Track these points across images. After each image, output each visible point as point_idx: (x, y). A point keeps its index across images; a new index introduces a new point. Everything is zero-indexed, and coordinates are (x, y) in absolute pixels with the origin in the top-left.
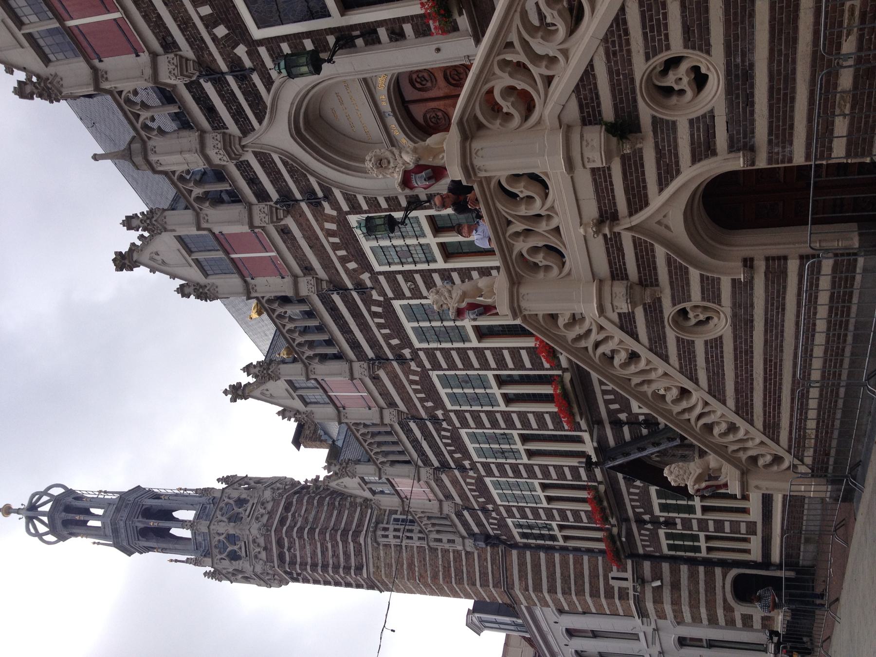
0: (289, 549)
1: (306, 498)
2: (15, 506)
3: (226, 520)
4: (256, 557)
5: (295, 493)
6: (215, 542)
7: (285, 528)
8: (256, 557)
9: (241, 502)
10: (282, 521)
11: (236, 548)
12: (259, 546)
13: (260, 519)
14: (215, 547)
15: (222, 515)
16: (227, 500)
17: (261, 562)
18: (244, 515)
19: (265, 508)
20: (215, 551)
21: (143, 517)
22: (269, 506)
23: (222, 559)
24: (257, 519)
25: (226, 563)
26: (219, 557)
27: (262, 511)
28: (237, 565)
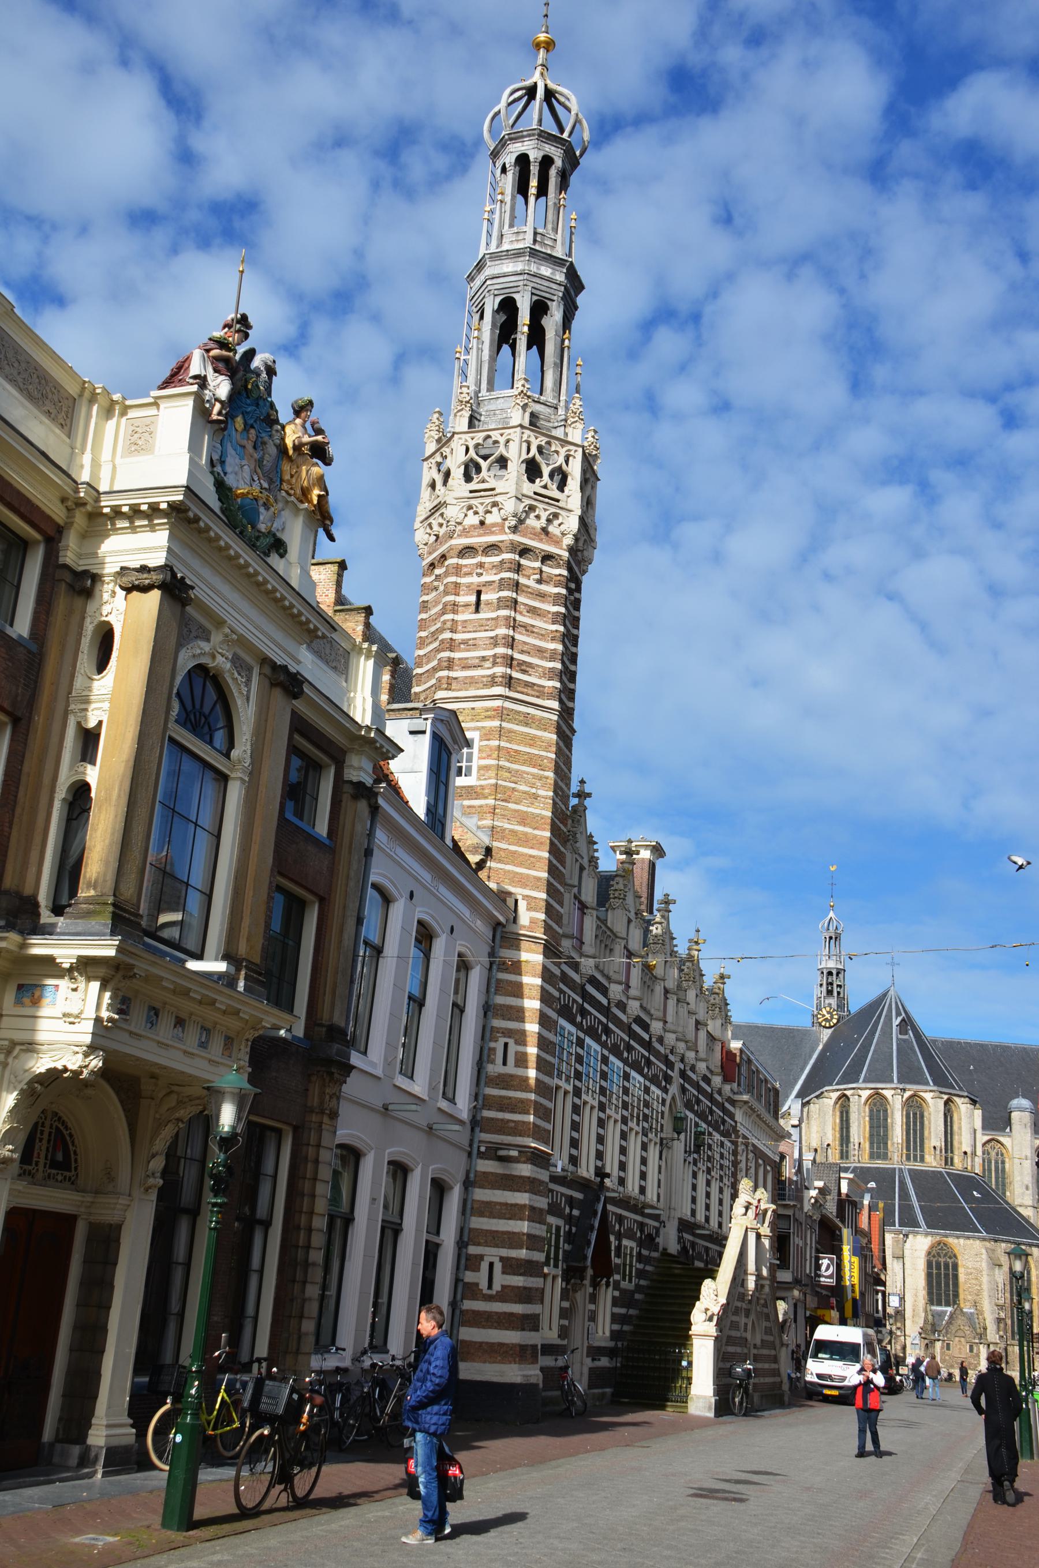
0: (481, 565)
3: (531, 455)
6: (495, 435)
7: (517, 557)
8: (470, 508)
9: (561, 477)
10: (525, 551)
11: (484, 473)
12: (488, 512)
19: (549, 521)
20: (479, 437)
21: (536, 301)
24: (532, 508)
27: (544, 516)
28: (458, 473)
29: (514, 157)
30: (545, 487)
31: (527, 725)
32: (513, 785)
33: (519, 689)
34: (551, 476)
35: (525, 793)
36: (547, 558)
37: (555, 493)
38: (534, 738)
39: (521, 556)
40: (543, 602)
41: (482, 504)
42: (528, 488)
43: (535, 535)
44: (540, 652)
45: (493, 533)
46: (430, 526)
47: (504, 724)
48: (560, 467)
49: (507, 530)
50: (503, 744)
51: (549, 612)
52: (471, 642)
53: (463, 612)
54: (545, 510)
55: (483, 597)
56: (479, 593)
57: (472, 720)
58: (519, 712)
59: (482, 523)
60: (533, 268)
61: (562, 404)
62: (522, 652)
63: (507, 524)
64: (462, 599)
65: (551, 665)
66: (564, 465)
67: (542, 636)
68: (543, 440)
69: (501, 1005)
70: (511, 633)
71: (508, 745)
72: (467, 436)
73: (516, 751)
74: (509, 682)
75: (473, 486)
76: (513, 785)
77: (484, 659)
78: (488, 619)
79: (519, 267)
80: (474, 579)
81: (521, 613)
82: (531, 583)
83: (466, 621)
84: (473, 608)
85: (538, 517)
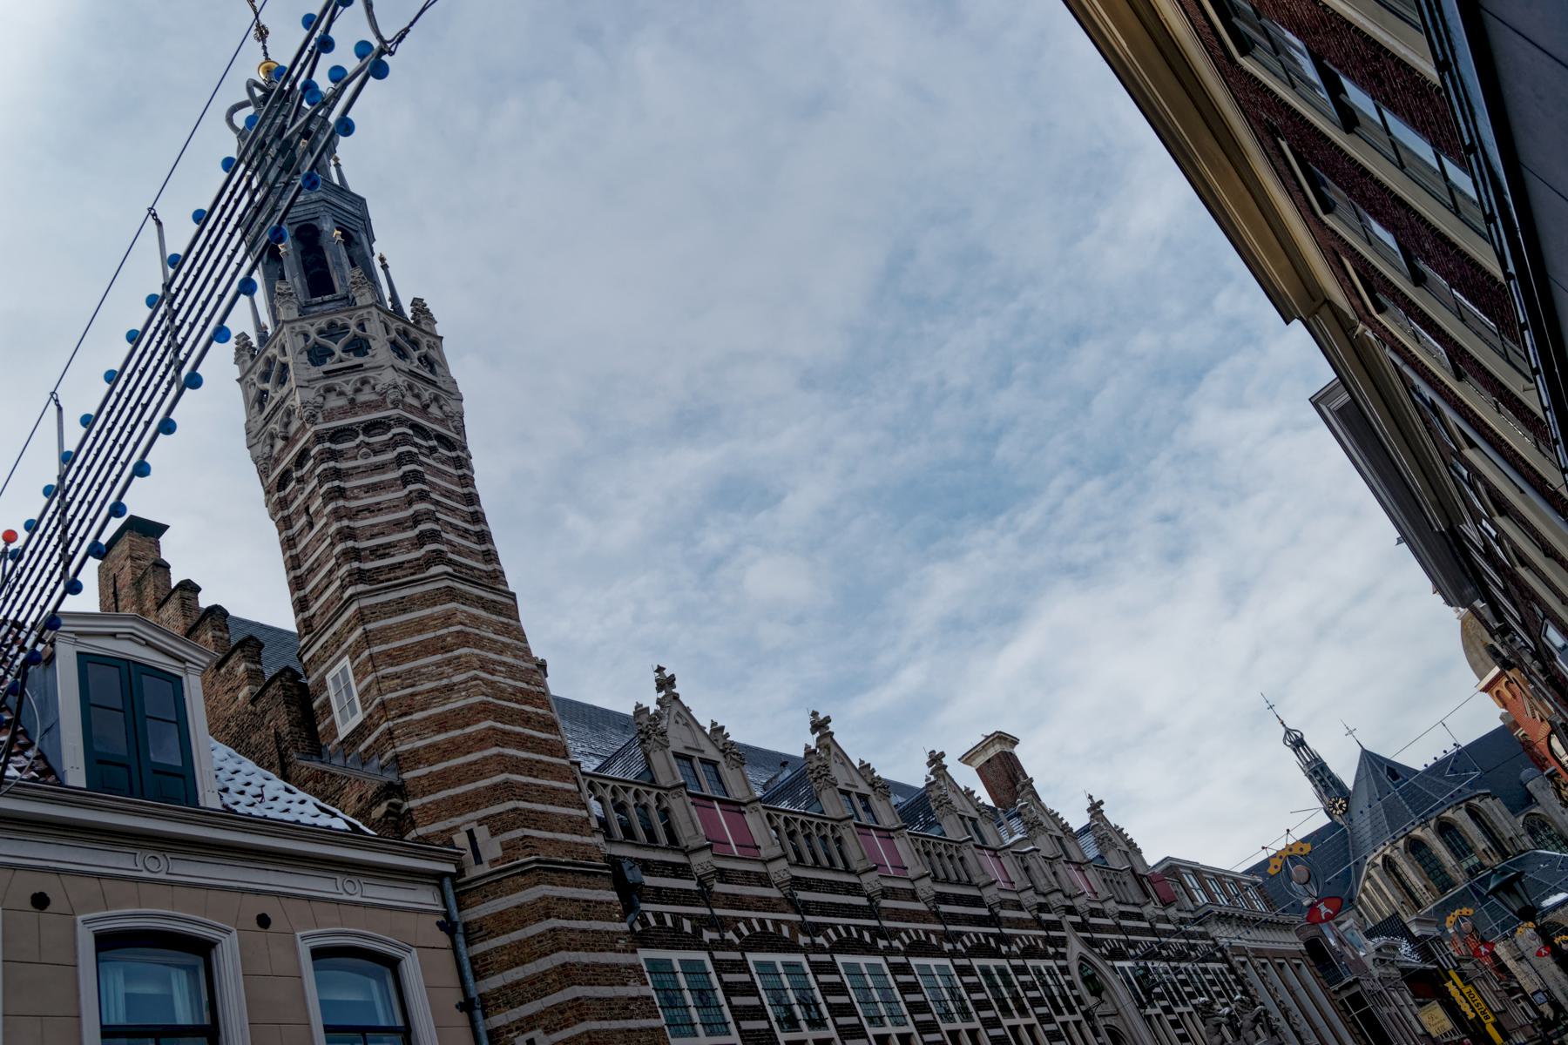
3: (311, 341)
4: (272, 436)
7: (327, 445)
9: (359, 346)
10: (338, 435)
12: (287, 425)
13: (332, 397)
16: (352, 324)
18: (329, 366)
19: (358, 391)
27: (349, 389)
31: (404, 611)
32: (410, 690)
35: (432, 690)
36: (371, 427)
38: (421, 621)
42: (316, 372)
43: (344, 412)
44: (399, 525)
47: (370, 626)
50: (376, 649)
54: (347, 382)
58: (388, 602)
66: (359, 332)
67: (395, 508)
68: (322, 323)
69: (499, 990)
70: (345, 523)
73: (400, 648)
74: (360, 576)
76: (410, 690)
81: (356, 498)
85: (341, 394)
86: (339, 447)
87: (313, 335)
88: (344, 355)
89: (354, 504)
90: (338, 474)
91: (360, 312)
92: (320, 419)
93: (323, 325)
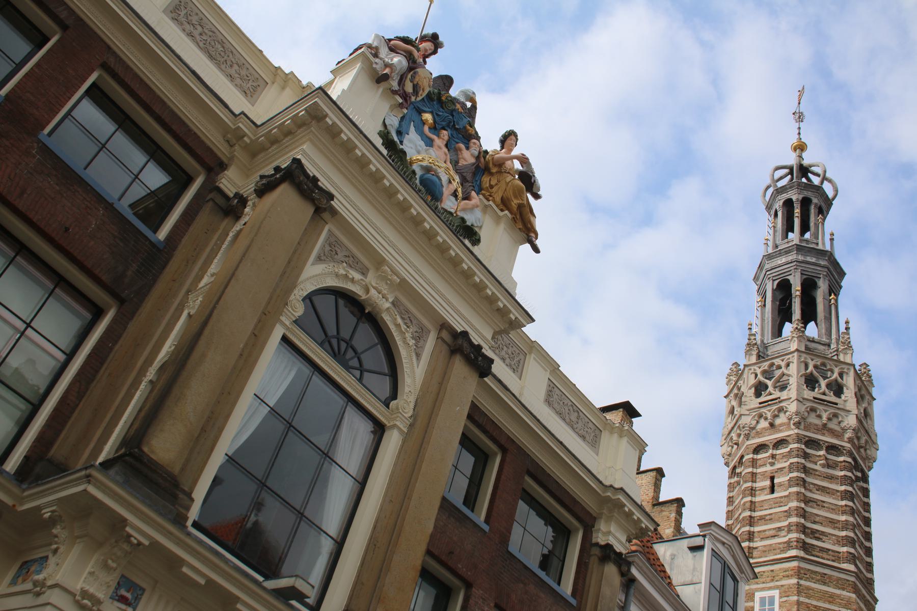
1: (849, 474)
2: (804, 155)
4: (760, 416)
5: (854, 459)
6: (777, 362)
7: (803, 447)
8: (760, 416)
9: (838, 389)
11: (770, 389)
12: (776, 416)
13: (813, 415)
14: (772, 365)
15: (815, 367)
17: (754, 422)
18: (816, 393)
19: (829, 419)
20: (765, 366)
21: (805, 279)
22: (833, 425)
23: (756, 375)
24: (813, 410)
25: (752, 381)
26: (759, 371)
27: (825, 416)
29: (781, 203)
30: (824, 394)
31: (825, 584)
33: (814, 553)
34: (829, 386)
36: (832, 448)
37: (833, 398)
39: (807, 446)
40: (831, 483)
41: (769, 411)
42: (808, 394)
44: (833, 523)
45: (781, 431)
46: (731, 439)
47: (802, 582)
48: (836, 380)
49: (793, 427)
50: (802, 599)
51: (838, 491)
52: (768, 517)
53: (760, 495)
55: (776, 481)
56: (772, 478)
57: (772, 580)
59: (772, 425)
60: (800, 258)
61: (834, 341)
62: (815, 522)
63: (792, 422)
64: (758, 485)
65: (844, 533)
66: (839, 379)
68: (818, 362)
71: (807, 601)
72: (756, 367)
75: (762, 399)
77: (779, 529)
78: (781, 497)
79: (790, 258)
80: (768, 468)
81: (811, 491)
82: (818, 467)
83: (762, 501)
84: (768, 490)
85: (820, 417)
86: (808, 451)
87: (811, 368)
88: (827, 391)
89: (809, 494)
90: (805, 470)
91: (844, 366)
92: (802, 427)
93: (819, 363)
